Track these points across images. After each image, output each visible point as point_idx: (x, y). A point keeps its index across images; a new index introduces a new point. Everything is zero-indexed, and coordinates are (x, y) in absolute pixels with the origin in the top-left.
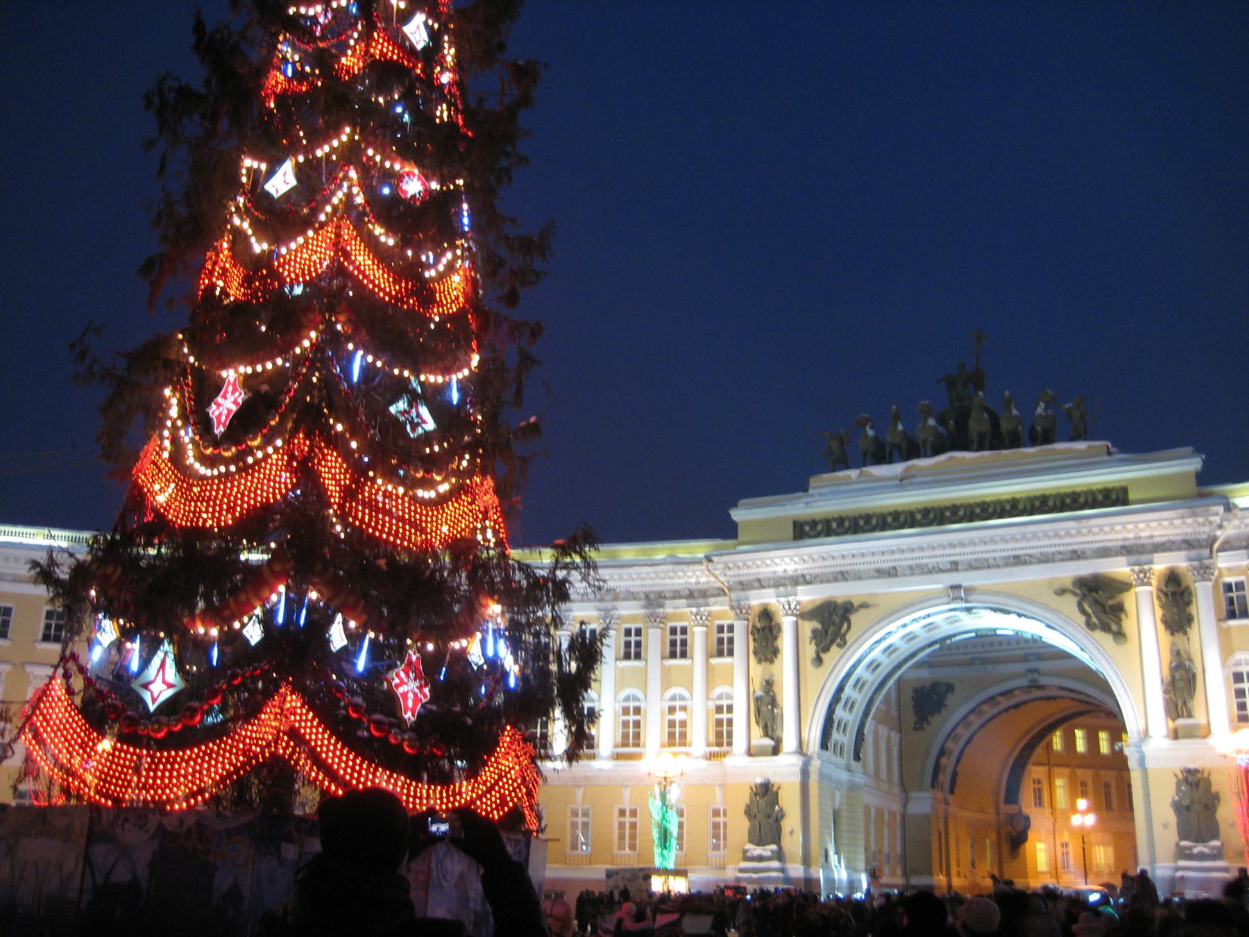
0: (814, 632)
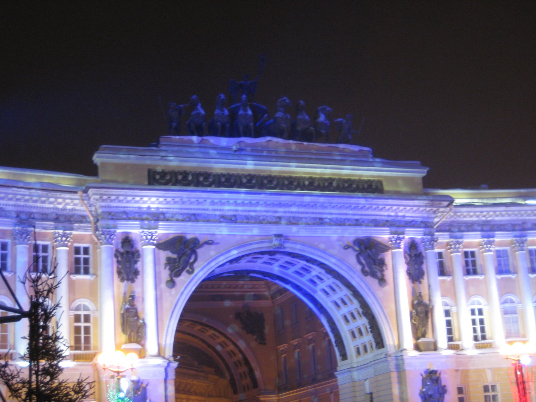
0: (169, 260)
